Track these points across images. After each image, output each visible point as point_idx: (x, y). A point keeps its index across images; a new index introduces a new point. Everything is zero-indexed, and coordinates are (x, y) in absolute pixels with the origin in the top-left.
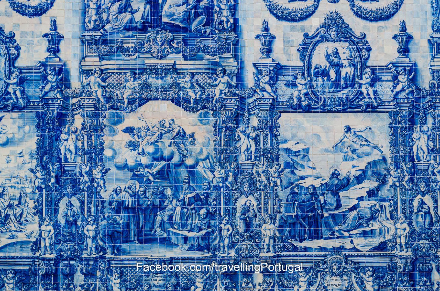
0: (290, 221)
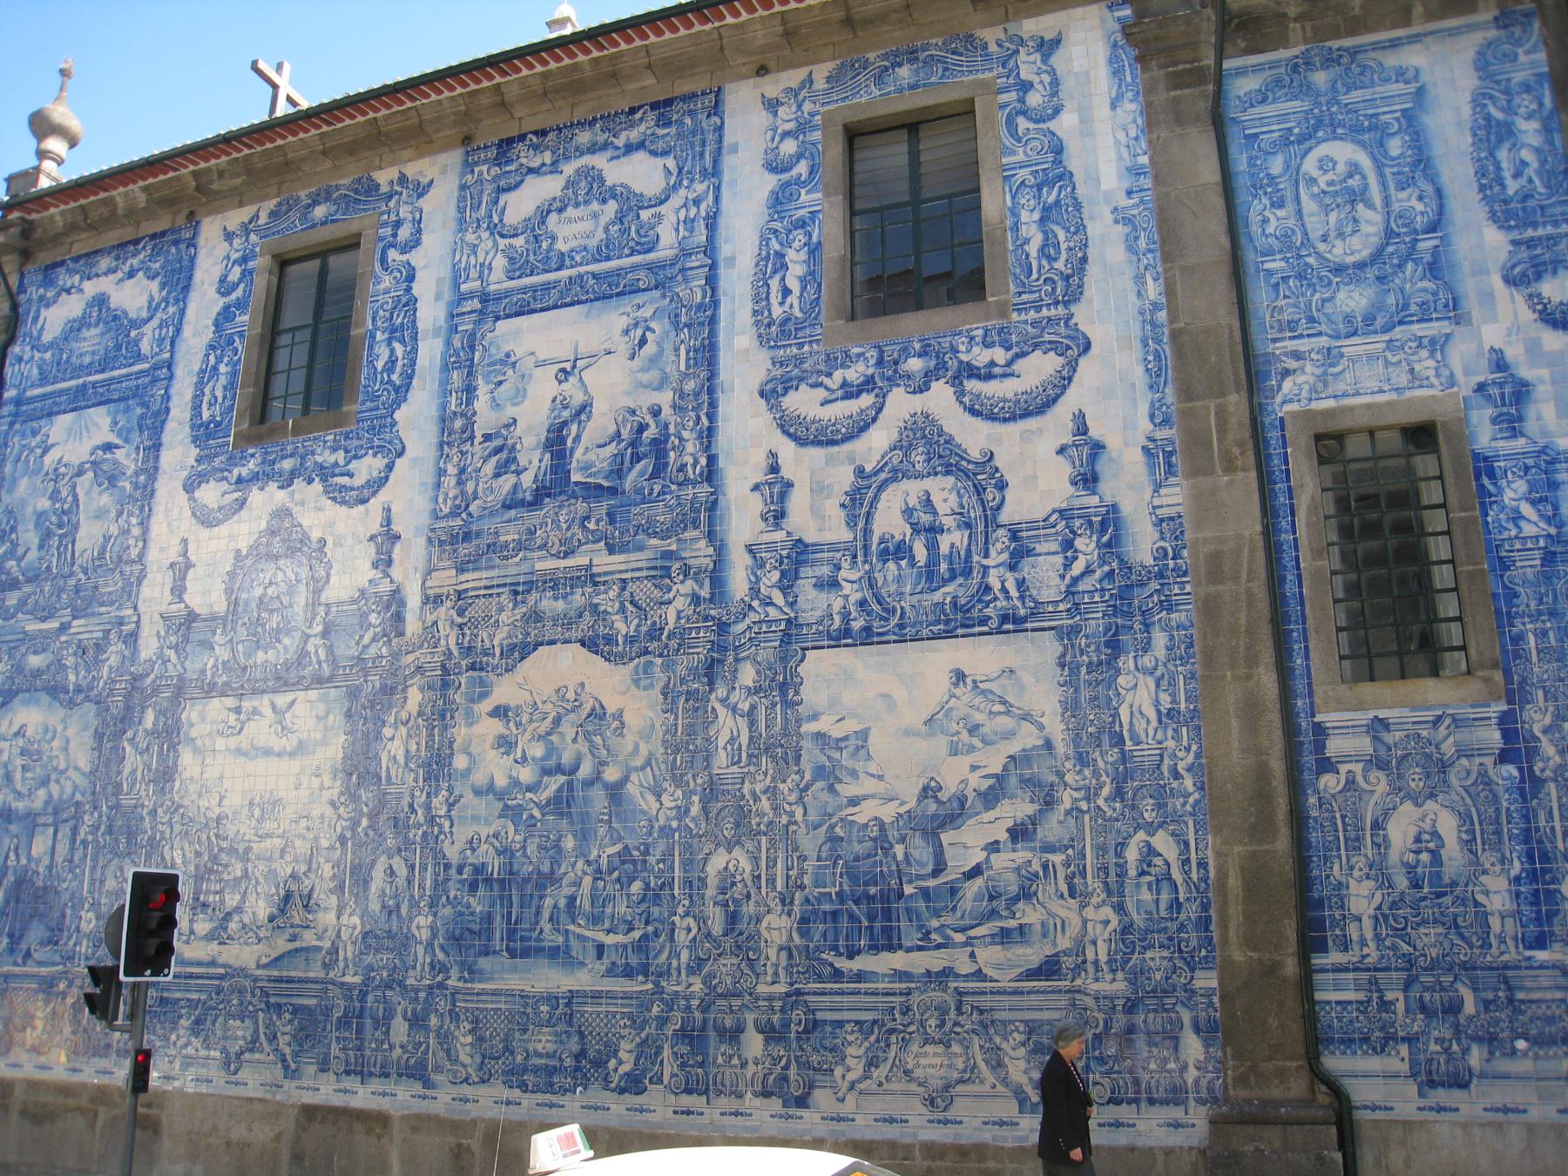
0: (827, 907)
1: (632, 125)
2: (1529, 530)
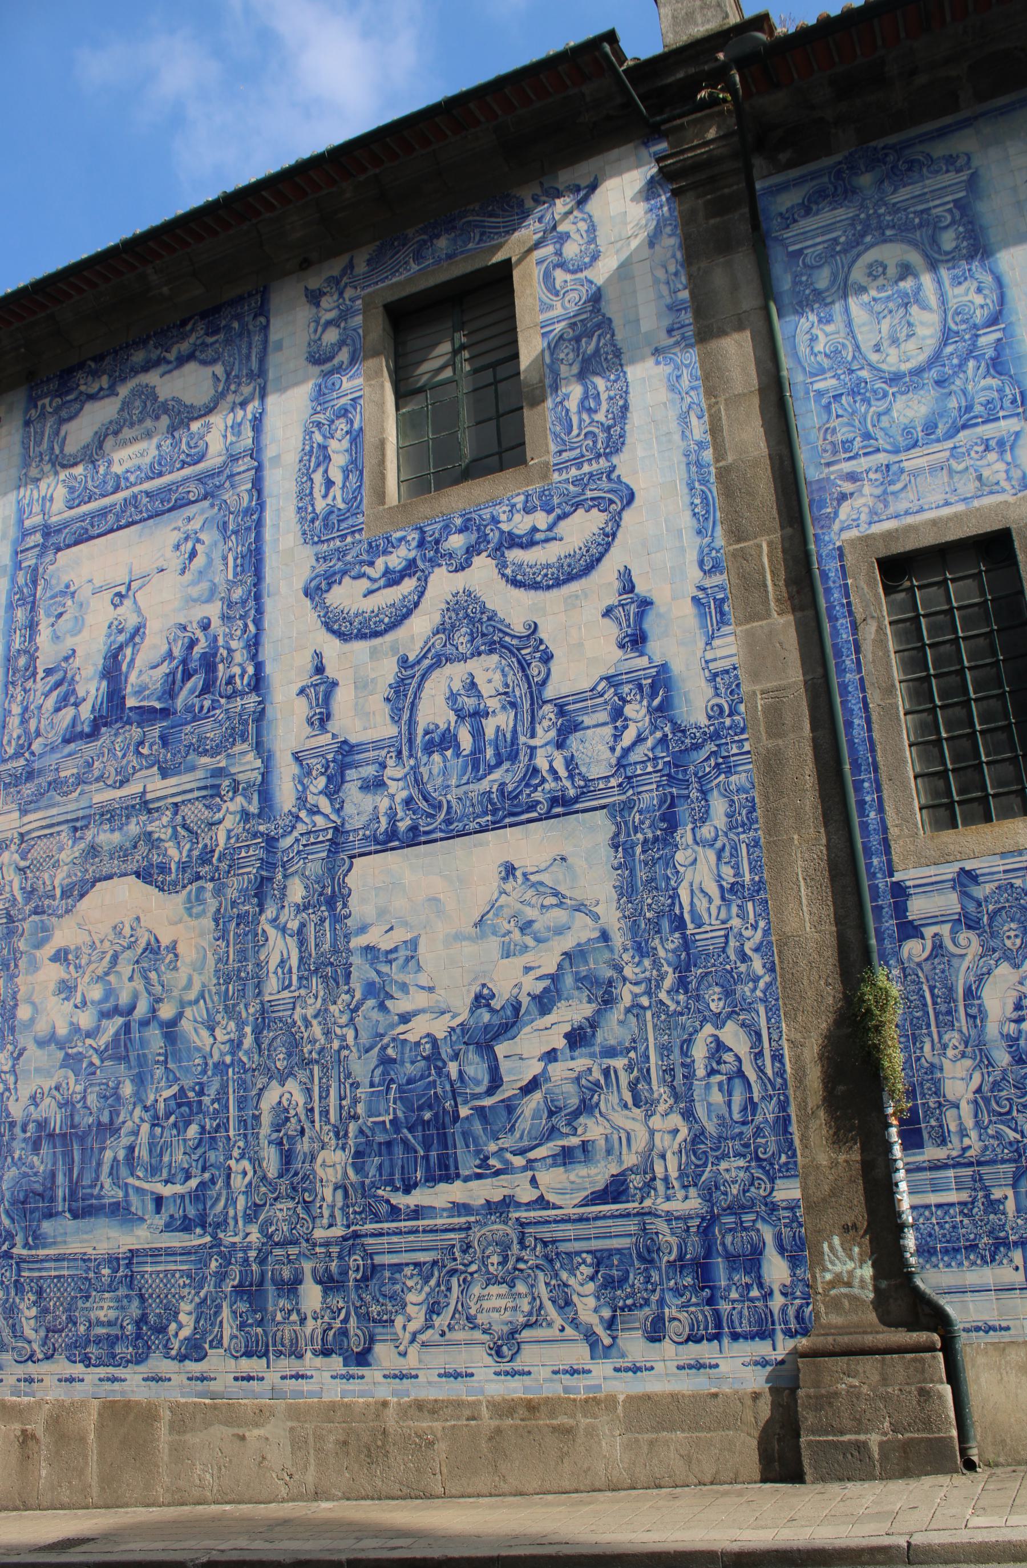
0: (381, 1138)
1: (184, 337)
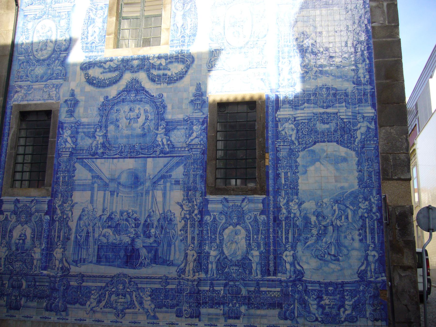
2: (68, 145)
